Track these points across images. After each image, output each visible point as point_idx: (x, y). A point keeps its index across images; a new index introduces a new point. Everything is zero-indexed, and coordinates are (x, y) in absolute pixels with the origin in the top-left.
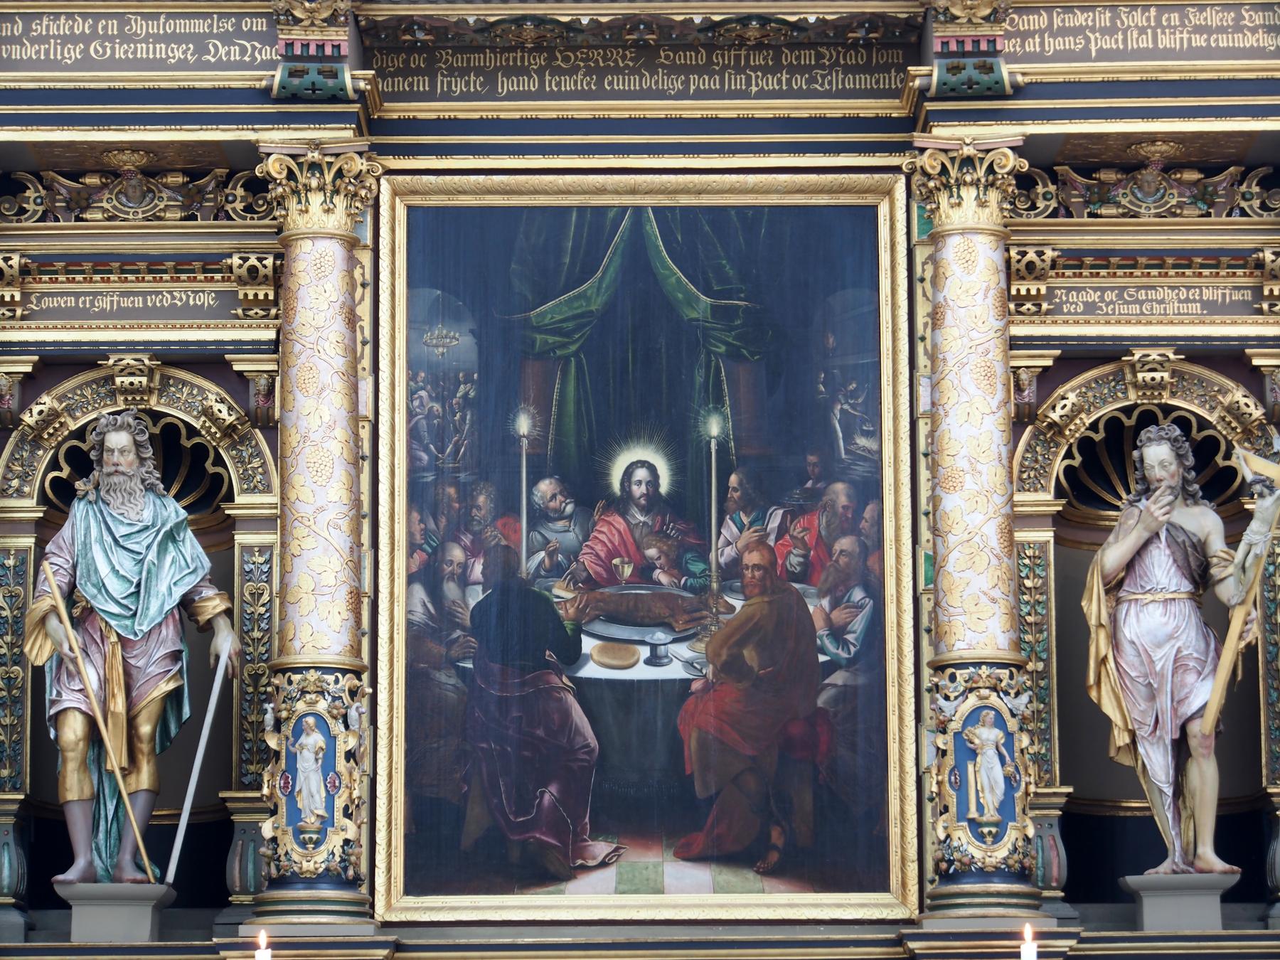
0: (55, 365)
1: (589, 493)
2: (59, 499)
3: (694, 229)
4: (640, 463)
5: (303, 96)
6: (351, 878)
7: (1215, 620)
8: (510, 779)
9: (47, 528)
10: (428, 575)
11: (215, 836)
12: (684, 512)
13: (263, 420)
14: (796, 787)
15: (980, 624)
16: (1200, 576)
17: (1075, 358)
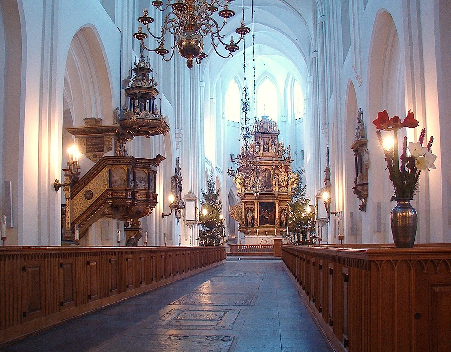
0: (247, 208)
1: (265, 212)
2: (248, 212)
3: (268, 203)
4: (267, 211)
5: (256, 199)
6: (257, 225)
7: (285, 217)
8: (262, 221)
9: (247, 213)
10: (259, 215)
11: (253, 223)
12: (268, 212)
13: (254, 209)
14: (272, 222)
15: (277, 217)
16: (284, 215)
17: (281, 207)
